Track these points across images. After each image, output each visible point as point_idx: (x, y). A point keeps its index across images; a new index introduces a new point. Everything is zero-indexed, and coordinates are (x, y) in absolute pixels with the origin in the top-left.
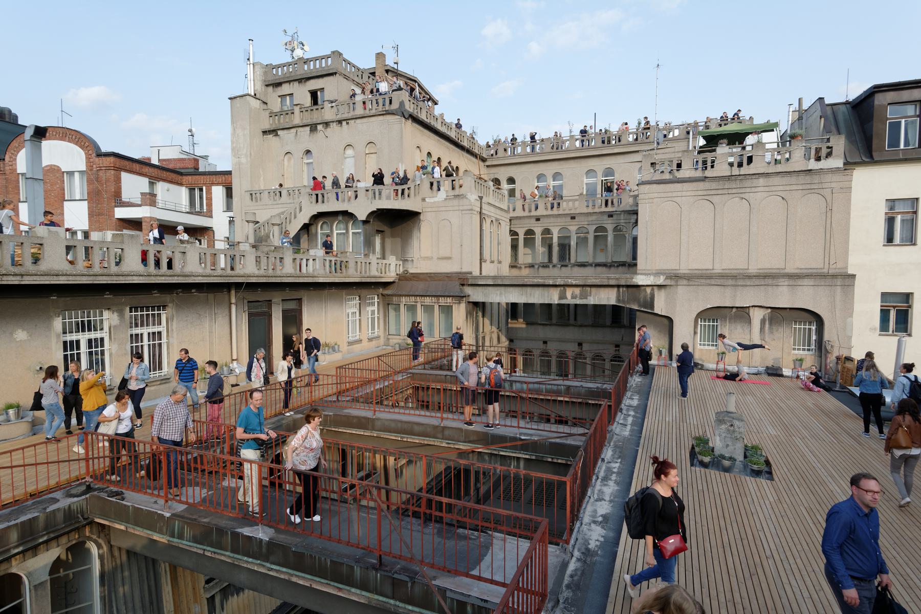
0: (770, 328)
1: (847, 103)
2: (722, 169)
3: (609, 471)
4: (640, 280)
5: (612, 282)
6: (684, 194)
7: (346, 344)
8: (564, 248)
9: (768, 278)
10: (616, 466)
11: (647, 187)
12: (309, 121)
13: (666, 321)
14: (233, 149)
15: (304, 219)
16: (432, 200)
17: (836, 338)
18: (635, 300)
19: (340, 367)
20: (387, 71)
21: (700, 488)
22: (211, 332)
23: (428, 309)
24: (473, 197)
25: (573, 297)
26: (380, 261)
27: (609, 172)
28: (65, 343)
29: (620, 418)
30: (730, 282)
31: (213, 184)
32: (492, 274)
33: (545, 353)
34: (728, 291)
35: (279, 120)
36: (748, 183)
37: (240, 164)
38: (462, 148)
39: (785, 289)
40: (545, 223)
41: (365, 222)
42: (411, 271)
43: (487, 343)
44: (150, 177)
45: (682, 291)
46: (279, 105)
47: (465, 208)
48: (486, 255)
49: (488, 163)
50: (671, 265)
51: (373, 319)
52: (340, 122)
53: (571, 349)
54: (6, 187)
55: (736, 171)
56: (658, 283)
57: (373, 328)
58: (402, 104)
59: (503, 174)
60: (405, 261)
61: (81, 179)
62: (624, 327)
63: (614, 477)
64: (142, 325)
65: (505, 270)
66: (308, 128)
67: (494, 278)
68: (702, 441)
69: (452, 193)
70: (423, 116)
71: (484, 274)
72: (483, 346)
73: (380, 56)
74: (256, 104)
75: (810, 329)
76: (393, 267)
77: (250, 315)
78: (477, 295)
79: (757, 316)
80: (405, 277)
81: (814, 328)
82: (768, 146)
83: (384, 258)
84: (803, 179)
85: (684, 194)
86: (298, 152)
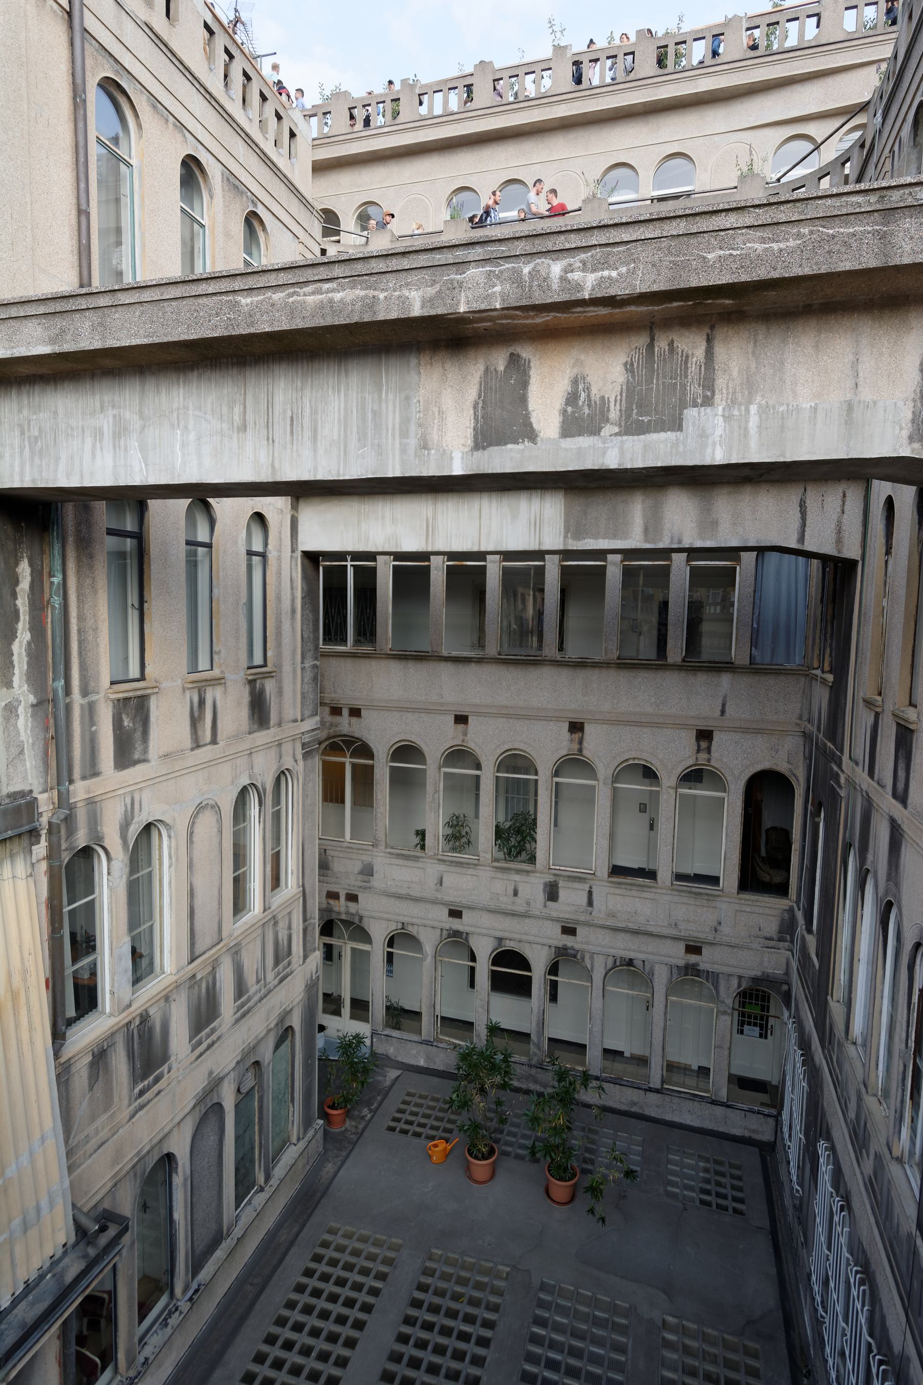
33: (459, 755)
53: (547, 745)
62: (727, 667)
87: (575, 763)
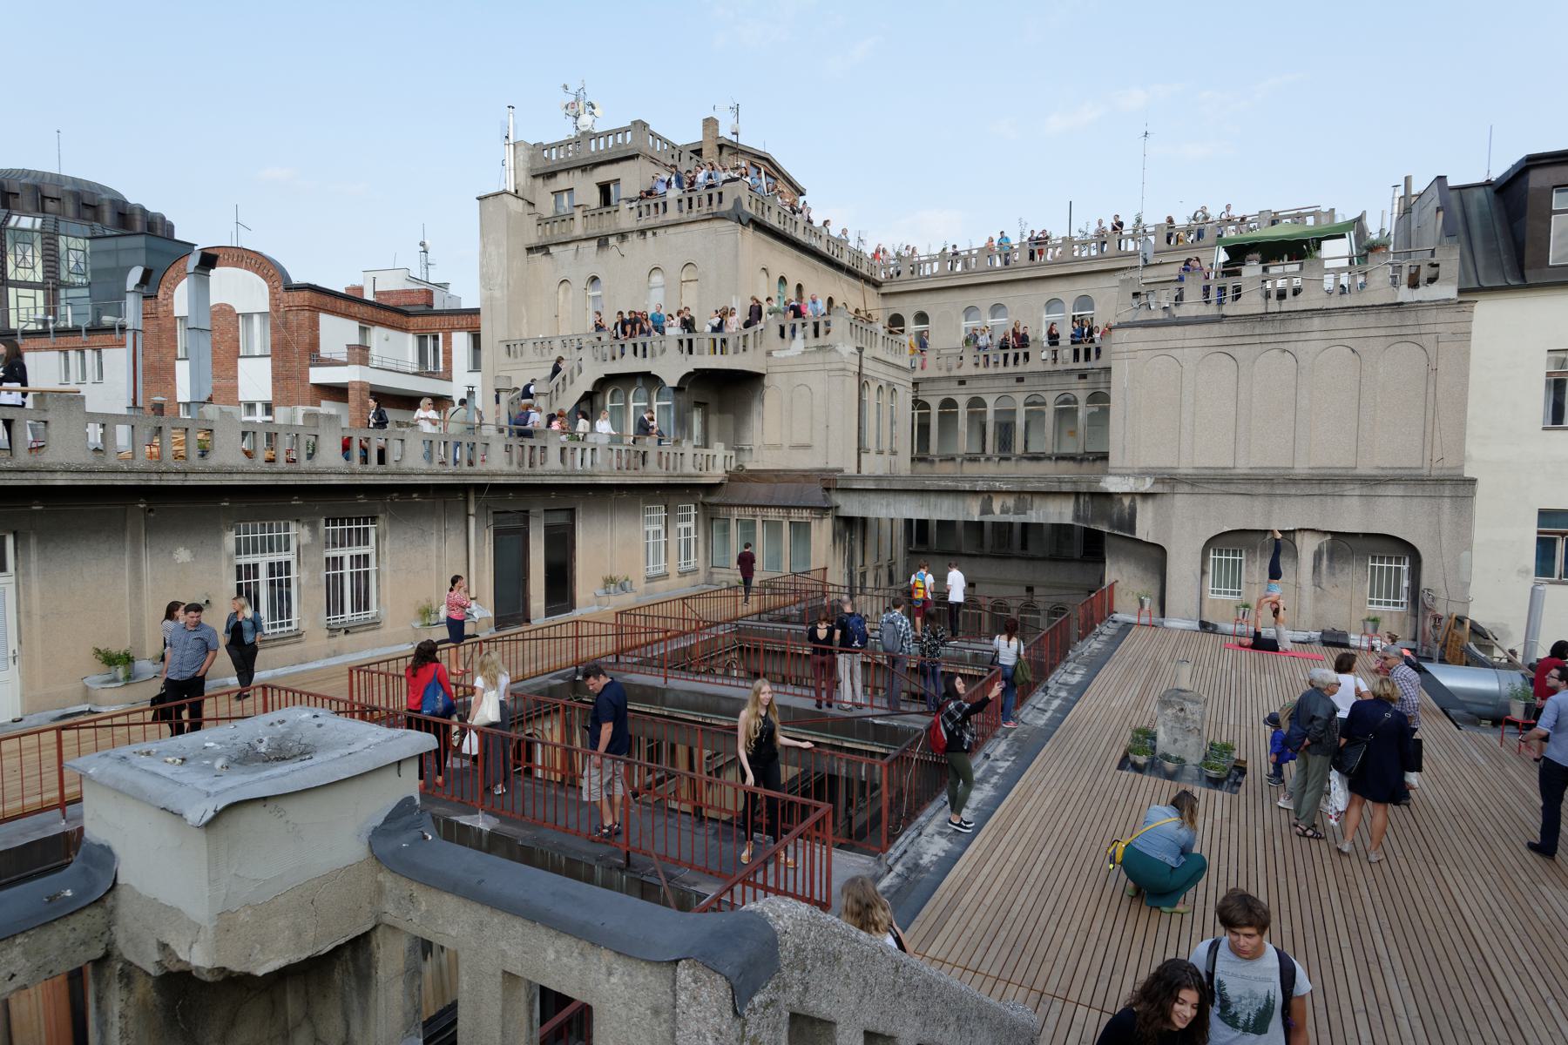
0: (1330, 567)
1: (1488, 184)
2: (1251, 303)
3: (991, 771)
4: (1112, 484)
5: (1066, 488)
6: (1187, 343)
7: (643, 581)
8: (1006, 430)
9: (1327, 482)
10: (1003, 765)
11: (1127, 332)
12: (596, 232)
13: (1155, 553)
14: (482, 277)
15: (585, 384)
16: (783, 354)
17: (1441, 585)
18: (1105, 517)
19: (622, 613)
20: (721, 147)
21: (1116, 797)
22: (439, 557)
23: (773, 527)
24: (846, 349)
25: (1004, 511)
26: (698, 451)
27: (1085, 301)
28: (239, 567)
29: (1038, 699)
30: (1262, 489)
31: (454, 329)
32: (880, 472)
34: (1259, 505)
35: (552, 230)
36: (1293, 326)
37: (491, 298)
38: (839, 267)
39: (1354, 502)
40: (974, 388)
41: (678, 390)
42: (749, 466)
43: (870, 583)
44: (361, 320)
45: (1182, 503)
46: (552, 206)
47: (834, 366)
48: (871, 442)
49: (883, 290)
50: (1163, 459)
51: (688, 542)
52: (643, 232)
54: (159, 338)
55: (1274, 305)
56: (1142, 490)
57: (687, 556)
58: (738, 202)
59: (907, 308)
60: (739, 450)
61: (263, 324)
63: (994, 780)
64: (342, 545)
65: (903, 465)
66: (595, 243)
67: (878, 478)
68: (1145, 737)
69: (813, 342)
70: (773, 220)
71: (864, 472)
72: (863, 586)
73: (710, 124)
74: (517, 206)
75: (1398, 569)
76: (719, 461)
77: (497, 533)
78: (851, 507)
79: (1308, 546)
80: (739, 477)
81: (1405, 567)
82: (1328, 264)
83: (706, 446)
84: (1387, 318)
85: (1187, 343)
86: (580, 281)
87: (1029, 607)
